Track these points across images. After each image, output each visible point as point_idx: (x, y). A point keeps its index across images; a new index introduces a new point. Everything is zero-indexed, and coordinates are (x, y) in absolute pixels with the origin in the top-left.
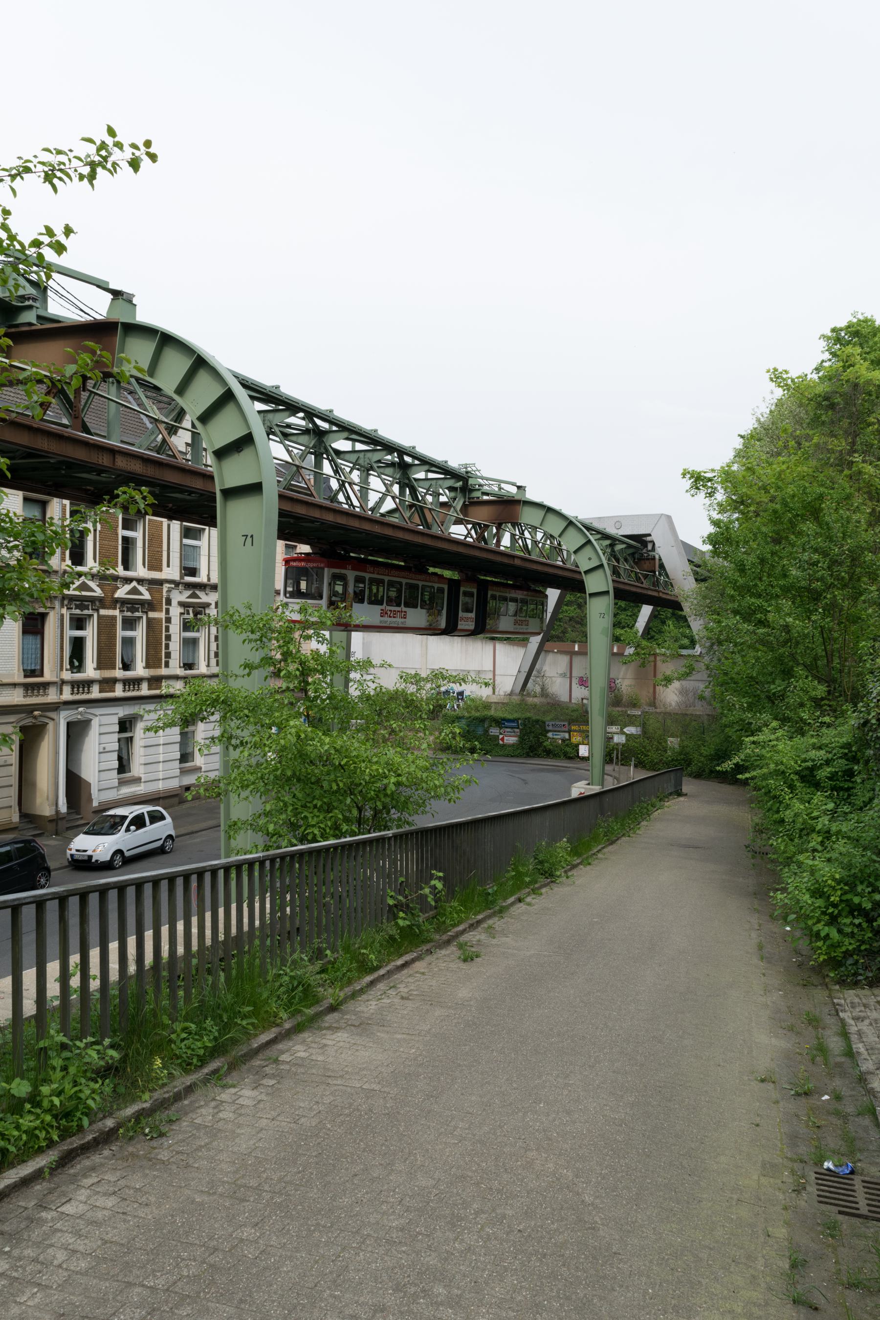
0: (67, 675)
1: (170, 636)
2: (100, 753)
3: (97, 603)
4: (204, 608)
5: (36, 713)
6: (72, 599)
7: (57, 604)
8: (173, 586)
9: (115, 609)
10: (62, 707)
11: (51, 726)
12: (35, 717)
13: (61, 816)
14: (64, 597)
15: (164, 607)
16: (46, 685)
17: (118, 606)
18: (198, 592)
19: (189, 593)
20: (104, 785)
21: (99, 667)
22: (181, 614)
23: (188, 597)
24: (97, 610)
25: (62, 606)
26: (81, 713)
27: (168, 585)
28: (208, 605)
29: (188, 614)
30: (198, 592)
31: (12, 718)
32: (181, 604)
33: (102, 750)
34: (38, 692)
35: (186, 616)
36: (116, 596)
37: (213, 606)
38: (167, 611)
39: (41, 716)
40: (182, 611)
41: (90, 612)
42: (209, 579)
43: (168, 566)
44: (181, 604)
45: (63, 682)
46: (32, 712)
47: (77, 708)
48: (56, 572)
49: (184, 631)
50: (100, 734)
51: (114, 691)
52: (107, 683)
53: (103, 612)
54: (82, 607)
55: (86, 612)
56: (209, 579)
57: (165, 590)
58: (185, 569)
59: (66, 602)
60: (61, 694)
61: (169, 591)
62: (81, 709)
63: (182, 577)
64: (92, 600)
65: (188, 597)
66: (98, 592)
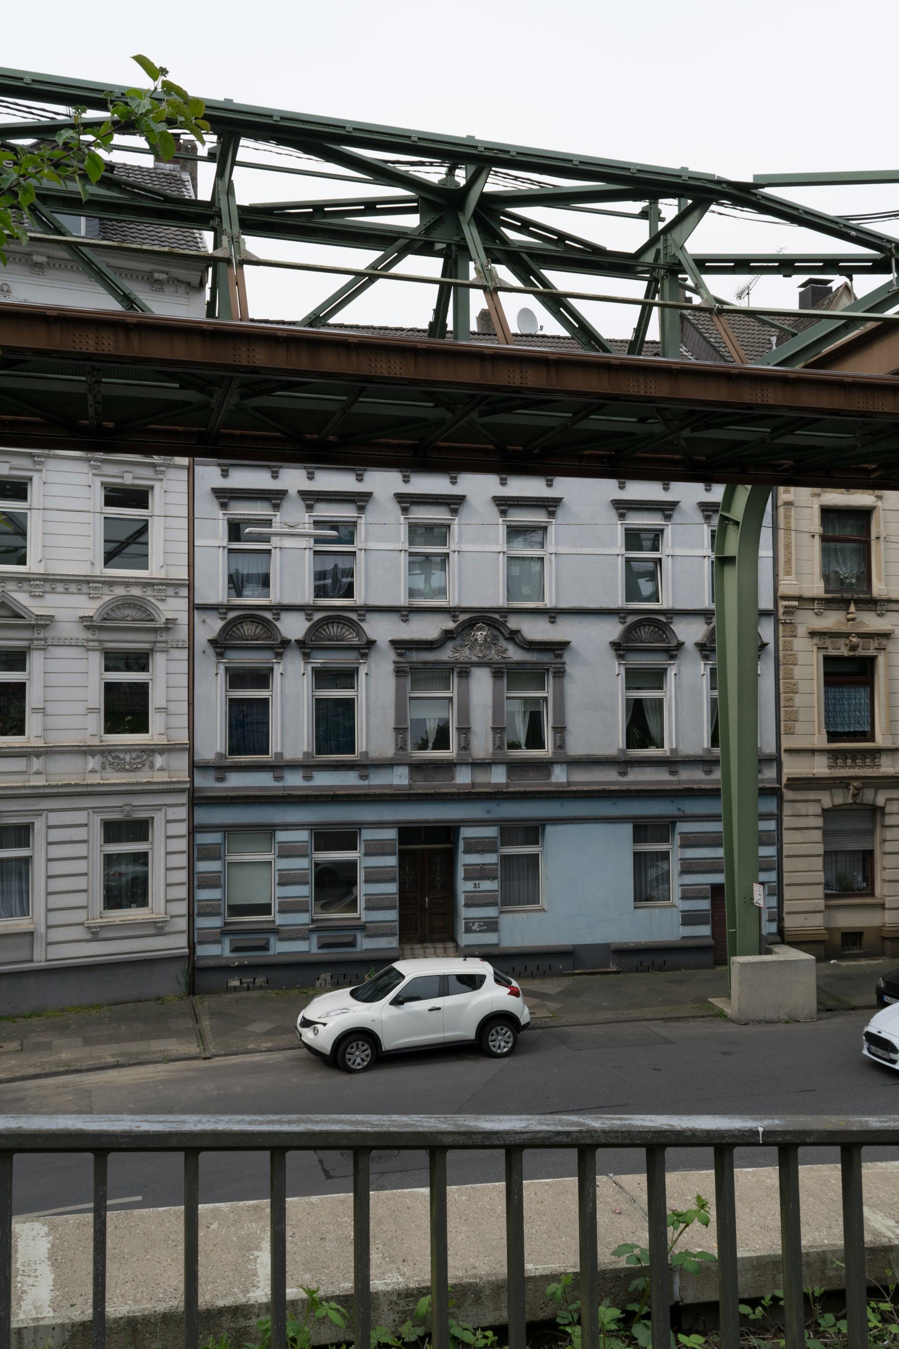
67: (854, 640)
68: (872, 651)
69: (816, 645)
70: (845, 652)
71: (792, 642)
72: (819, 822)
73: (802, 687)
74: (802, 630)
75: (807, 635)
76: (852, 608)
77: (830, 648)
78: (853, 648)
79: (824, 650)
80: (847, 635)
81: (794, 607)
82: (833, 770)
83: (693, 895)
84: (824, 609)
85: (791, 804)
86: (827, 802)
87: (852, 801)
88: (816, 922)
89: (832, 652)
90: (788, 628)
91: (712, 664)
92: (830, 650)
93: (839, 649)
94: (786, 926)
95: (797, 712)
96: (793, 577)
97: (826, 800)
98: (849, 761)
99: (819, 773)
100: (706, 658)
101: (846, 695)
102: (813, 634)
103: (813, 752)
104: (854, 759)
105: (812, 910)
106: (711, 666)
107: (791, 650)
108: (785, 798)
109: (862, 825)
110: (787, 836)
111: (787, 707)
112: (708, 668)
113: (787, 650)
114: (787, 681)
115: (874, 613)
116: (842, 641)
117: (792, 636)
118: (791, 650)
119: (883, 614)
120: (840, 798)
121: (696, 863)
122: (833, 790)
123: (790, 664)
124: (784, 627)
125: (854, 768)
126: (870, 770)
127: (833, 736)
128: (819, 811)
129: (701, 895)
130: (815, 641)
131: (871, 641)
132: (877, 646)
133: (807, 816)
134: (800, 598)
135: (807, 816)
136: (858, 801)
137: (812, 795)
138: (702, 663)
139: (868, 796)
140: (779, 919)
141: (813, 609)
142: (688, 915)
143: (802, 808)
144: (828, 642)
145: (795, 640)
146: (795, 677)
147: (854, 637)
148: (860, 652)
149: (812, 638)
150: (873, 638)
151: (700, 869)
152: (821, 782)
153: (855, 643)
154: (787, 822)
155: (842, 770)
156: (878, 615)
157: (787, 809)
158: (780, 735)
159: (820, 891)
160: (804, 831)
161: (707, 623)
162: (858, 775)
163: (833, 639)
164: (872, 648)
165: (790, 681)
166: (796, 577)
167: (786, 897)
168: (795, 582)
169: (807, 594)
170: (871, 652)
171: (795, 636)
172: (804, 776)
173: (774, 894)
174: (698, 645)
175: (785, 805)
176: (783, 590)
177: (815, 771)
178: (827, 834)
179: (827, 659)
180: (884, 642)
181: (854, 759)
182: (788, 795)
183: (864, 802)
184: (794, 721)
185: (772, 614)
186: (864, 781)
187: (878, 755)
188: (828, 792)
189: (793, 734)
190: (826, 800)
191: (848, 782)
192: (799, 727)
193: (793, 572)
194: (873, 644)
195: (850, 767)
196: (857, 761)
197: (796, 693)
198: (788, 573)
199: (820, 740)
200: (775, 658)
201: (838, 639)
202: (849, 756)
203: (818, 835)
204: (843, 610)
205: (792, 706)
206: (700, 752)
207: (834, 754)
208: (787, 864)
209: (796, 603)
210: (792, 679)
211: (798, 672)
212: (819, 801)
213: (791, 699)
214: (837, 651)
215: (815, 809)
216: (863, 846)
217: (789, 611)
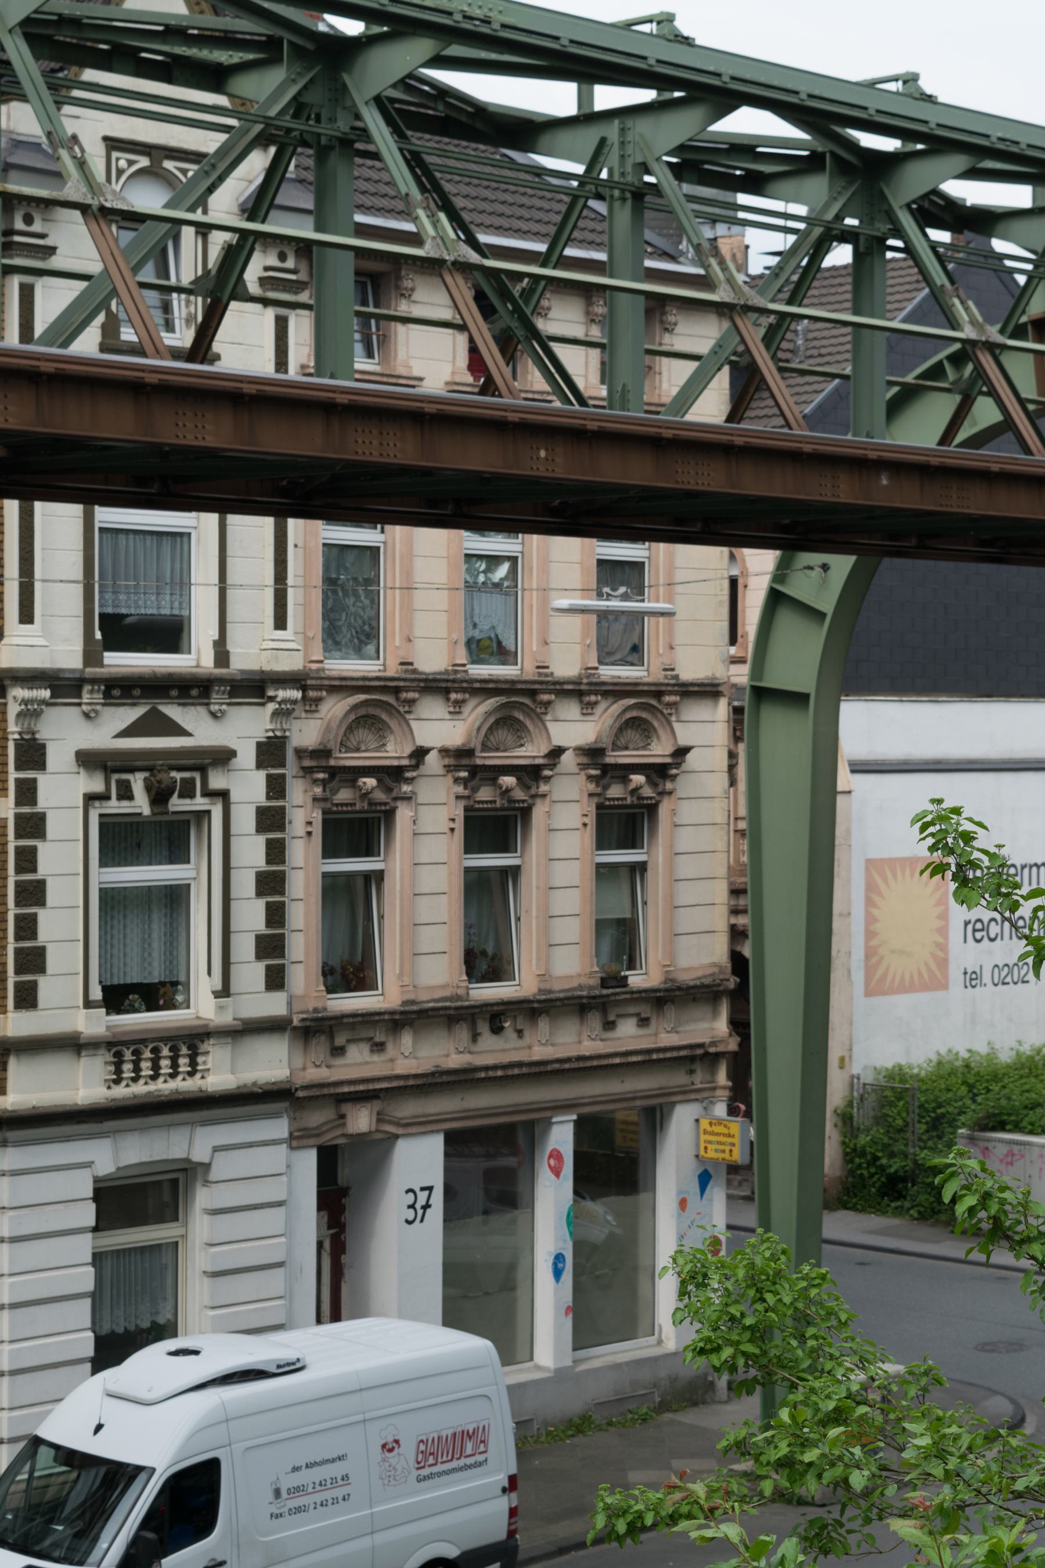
1: (41, 885)
4: (203, 770)
8: (46, 694)
15: (13, 775)
18: (173, 711)
19: (130, 715)
22: (90, 798)
23: (128, 732)
27: (18, 693)
28: (223, 757)
29: (126, 793)
30: (173, 711)
32: (88, 760)
35: (115, 806)
37: (247, 756)
38: (27, 792)
40: (97, 785)
42: (222, 656)
43: (27, 616)
44: (88, 760)
49: (103, 863)
56: (222, 656)
57: (13, 709)
58: (110, 622)
61: (31, 713)
63: (91, 657)
65: (129, 732)
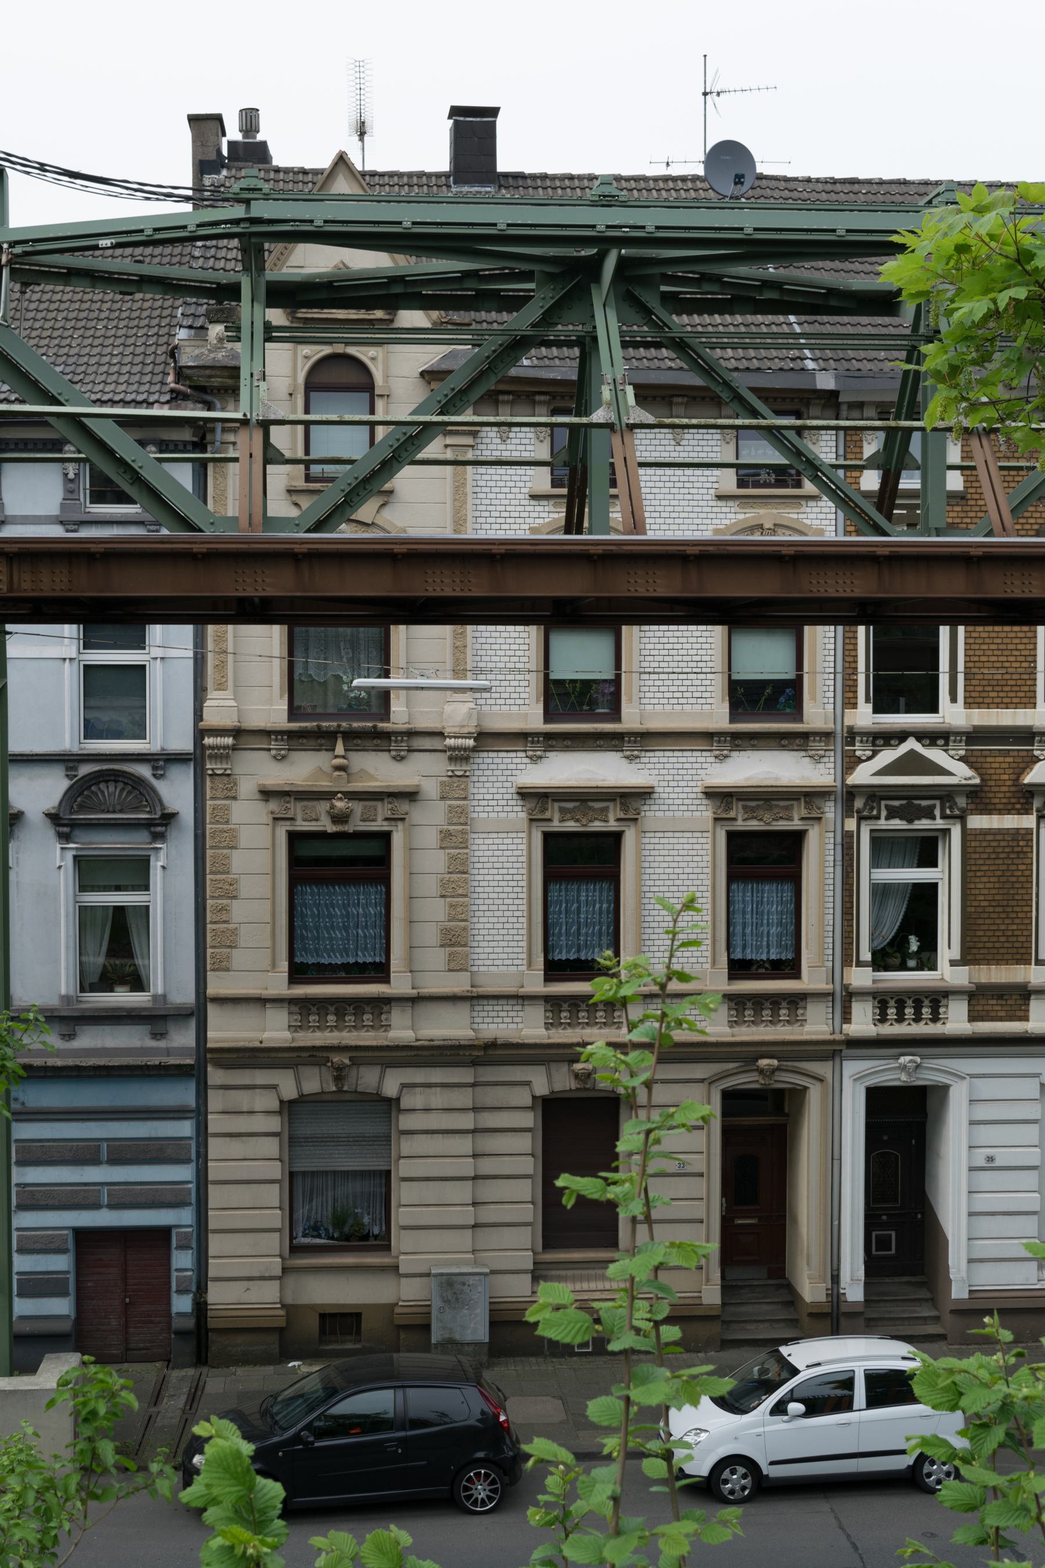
0: (861, 977)
2: (971, 1169)
3: (962, 802)
5: (763, 1062)
6: (874, 795)
7: (831, 811)
9: (1028, 812)
10: (846, 1052)
11: (814, 1095)
12: (761, 1071)
13: (844, 1309)
14: (851, 793)
16: (796, 1001)
17: (1037, 803)
20: (987, 1248)
21: (968, 957)
24: (962, 819)
25: (848, 811)
26: (903, 1068)
31: (701, 1071)
33: (982, 1163)
34: (775, 1013)
36: (1029, 778)
39: (778, 1069)
41: (939, 823)
45: (850, 995)
46: (757, 1059)
47: (897, 1057)
48: (827, 736)
50: (972, 1123)
51: (1026, 1019)
52: (1001, 997)
53: (978, 822)
54: (910, 813)
55: (923, 824)
59: (859, 803)
60: (847, 1018)
62: (903, 1060)
64: (946, 795)
66: (961, 773)
67: (340, 805)
68: (379, 822)
69: (272, 813)
70: (327, 825)
71: (228, 808)
72: (274, 1124)
73: (248, 887)
74: (247, 787)
75: (258, 796)
76: (340, 749)
77: (299, 817)
78: (339, 818)
79: (288, 823)
80: (327, 796)
81: (226, 747)
82: (300, 1034)
83: (38, 1246)
84: (289, 750)
85: (221, 1091)
86: (289, 1089)
87: (334, 1089)
88: (267, 1295)
89: (302, 826)
90: (220, 783)
91: (77, 849)
92: (299, 822)
93: (317, 820)
94: (209, 1301)
95: (234, 932)
96: (228, 694)
97: (288, 1085)
98: (331, 1018)
99: (269, 1039)
100: (64, 837)
101: (339, 899)
102: (267, 794)
103: (262, 1002)
104: (340, 1015)
105: (257, 1275)
106: (74, 853)
107: (227, 822)
108: (210, 1082)
109: (369, 1127)
110: (216, 1148)
111: (215, 923)
112: (69, 856)
113: (218, 823)
114: (218, 877)
115: (385, 756)
116: (323, 807)
117: (227, 798)
118: (227, 822)
119: (403, 758)
120: (314, 1082)
121: (44, 1192)
122: (301, 1069)
123: (224, 848)
124: (212, 782)
125: (340, 1030)
126: (372, 1034)
127: (298, 973)
128: (275, 1105)
129: (52, 1246)
130: (273, 805)
131: (379, 804)
132: (389, 814)
133: (251, 1112)
134: (237, 733)
135: (251, 1112)
136: (345, 1088)
137: (261, 1077)
138: (59, 846)
139: (367, 1079)
140: (199, 1287)
141: (269, 750)
142: (29, 1280)
143: (242, 1100)
144: (297, 809)
145: (235, 805)
146: (234, 871)
147: (341, 799)
148: (357, 825)
149: (267, 801)
150: (382, 800)
151: (51, 1202)
152: (273, 1055)
153: (341, 810)
154: (215, 1122)
155: (318, 1034)
156: (394, 758)
157: (215, 1101)
158: (205, 971)
159: (274, 1243)
160: (244, 1139)
161: (67, 776)
162: (345, 1042)
163: (305, 803)
164: (380, 818)
165: (224, 876)
166: (235, 693)
167: (212, 1252)
168: (233, 703)
169: (256, 721)
170: (378, 825)
171: (235, 798)
172: (241, 1044)
173: (188, 1247)
174: (50, 816)
175: (211, 1093)
176: (212, 718)
177: (266, 1035)
178: (293, 1142)
179: (294, 837)
180: (404, 806)
181: (340, 1015)
182: (215, 1076)
183: (360, 1089)
184: (230, 947)
185: (190, 760)
186: (354, 1054)
187: (386, 1008)
188: (292, 1071)
189: (227, 970)
190: (288, 1085)
191: (325, 1054)
192: (239, 958)
193: (230, 683)
194: (383, 810)
195: (332, 1028)
196: (347, 1018)
197: (235, 897)
198: (221, 687)
199: (278, 984)
200: (196, 836)
201: (315, 803)
202: (332, 1009)
203: (271, 1147)
204: (327, 750)
205: (225, 922)
206: (53, 1002)
207: (303, 1007)
208: (216, 1196)
209: (229, 741)
210: (228, 873)
211: (238, 861)
212: (274, 1087)
213: (223, 909)
214: (314, 823)
215: (268, 1101)
216: (376, 1164)
217: (223, 755)
